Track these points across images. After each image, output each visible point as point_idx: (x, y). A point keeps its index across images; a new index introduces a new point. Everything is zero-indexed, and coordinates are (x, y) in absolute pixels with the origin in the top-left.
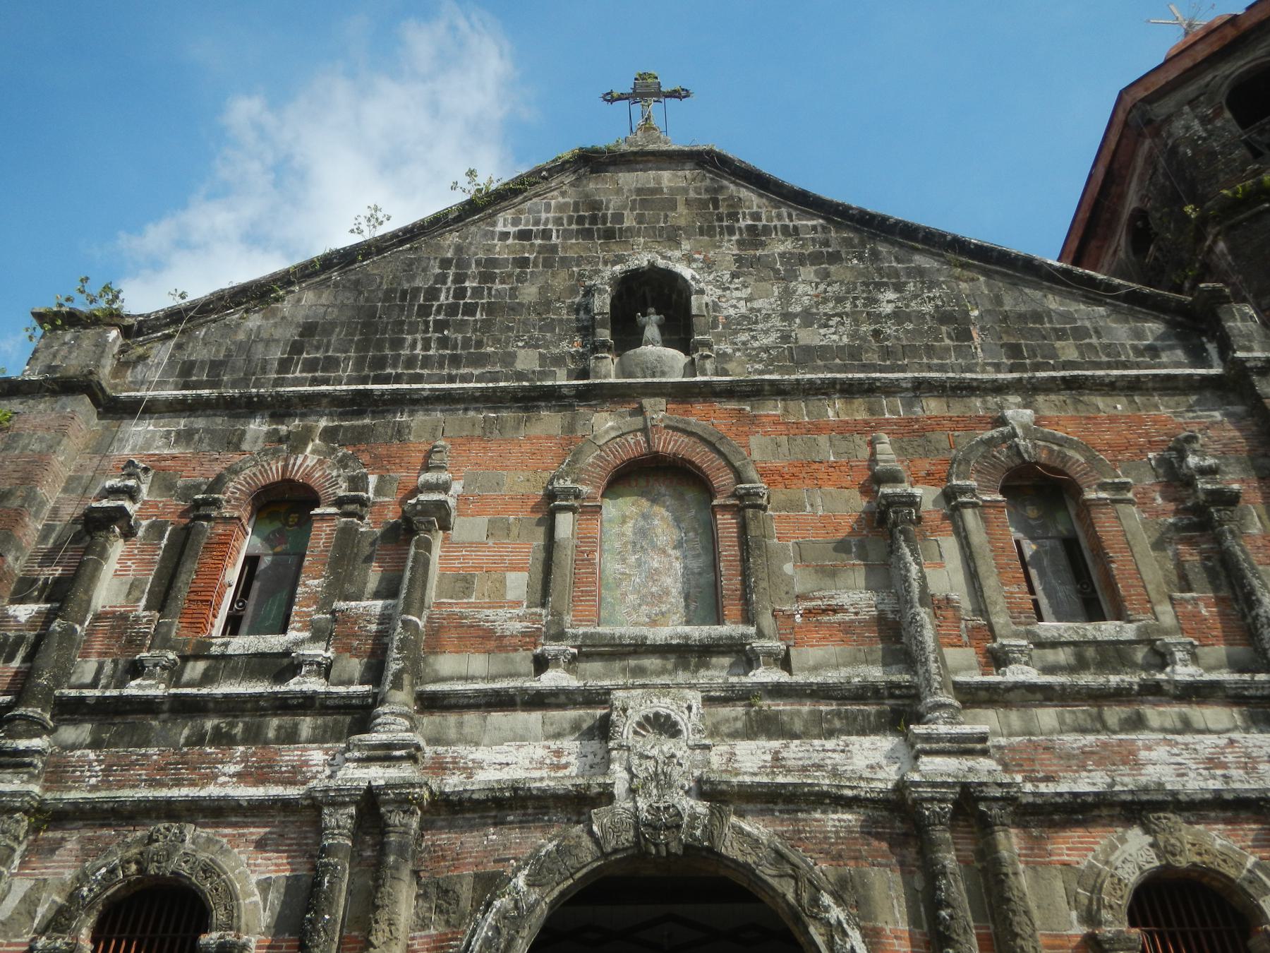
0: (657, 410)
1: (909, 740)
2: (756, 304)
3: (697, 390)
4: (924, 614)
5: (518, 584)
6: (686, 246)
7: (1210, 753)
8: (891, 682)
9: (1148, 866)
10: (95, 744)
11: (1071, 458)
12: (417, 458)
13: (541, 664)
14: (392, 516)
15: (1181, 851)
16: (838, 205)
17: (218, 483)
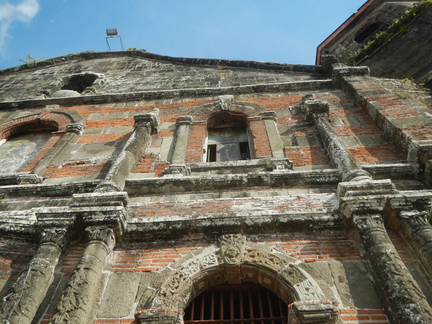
3: (76, 101)
7: (282, 204)
8: (86, 183)
9: (208, 266)
11: (247, 109)
15: (238, 254)
16: (179, 58)
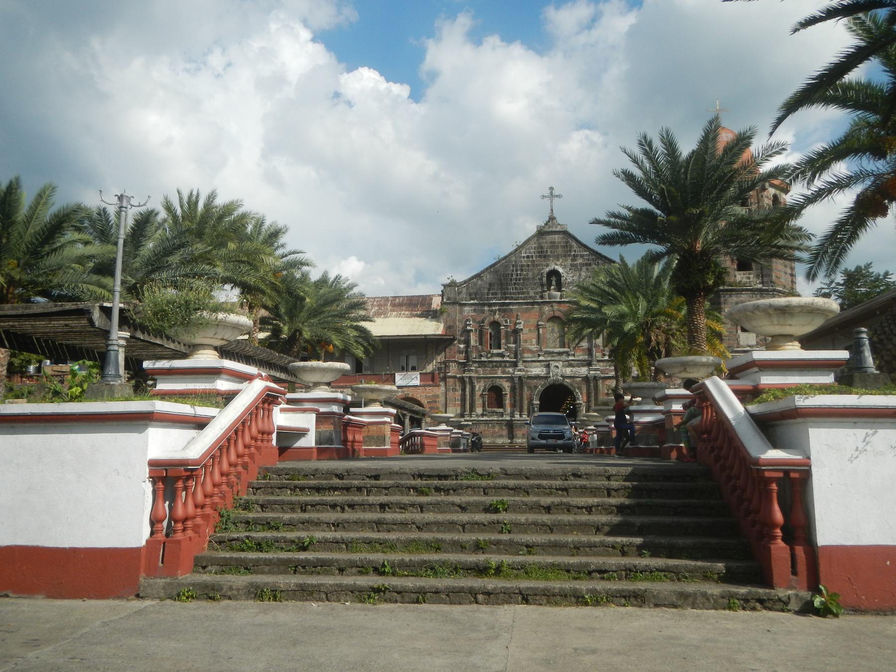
0: (556, 307)
1: (589, 369)
2: (574, 278)
4: (594, 349)
5: (534, 341)
6: (561, 261)
10: (479, 367)
12: (515, 316)
13: (539, 356)
14: (513, 328)
17: (483, 322)
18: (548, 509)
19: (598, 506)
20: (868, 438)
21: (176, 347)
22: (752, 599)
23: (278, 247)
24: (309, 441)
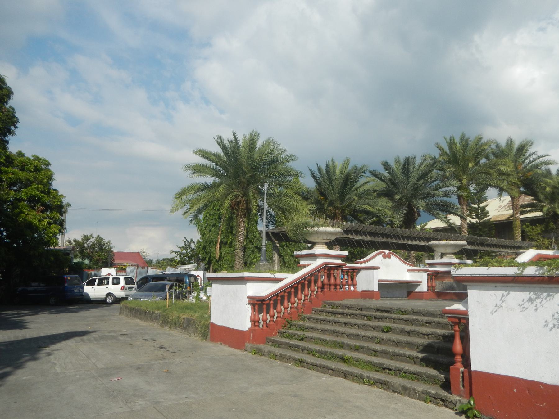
18: (409, 333)
19: (432, 334)
20: (504, 298)
21: (363, 238)
22: (438, 398)
23: (530, 155)
24: (423, 288)
